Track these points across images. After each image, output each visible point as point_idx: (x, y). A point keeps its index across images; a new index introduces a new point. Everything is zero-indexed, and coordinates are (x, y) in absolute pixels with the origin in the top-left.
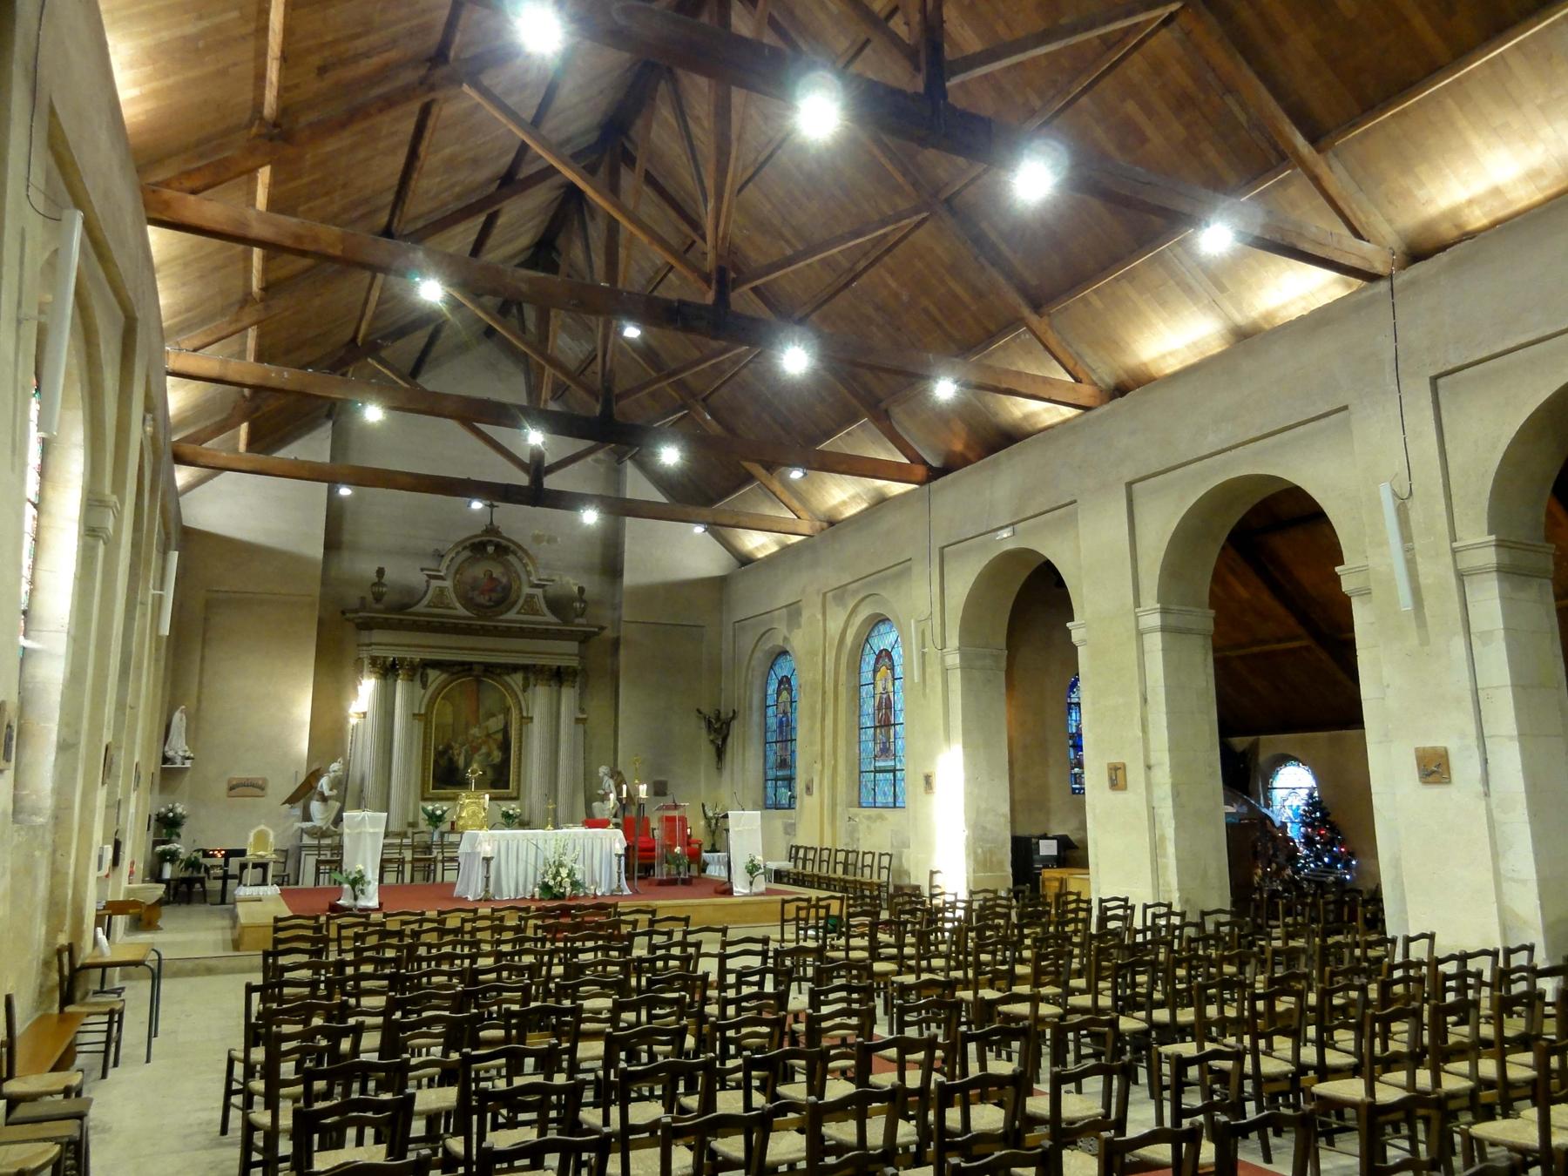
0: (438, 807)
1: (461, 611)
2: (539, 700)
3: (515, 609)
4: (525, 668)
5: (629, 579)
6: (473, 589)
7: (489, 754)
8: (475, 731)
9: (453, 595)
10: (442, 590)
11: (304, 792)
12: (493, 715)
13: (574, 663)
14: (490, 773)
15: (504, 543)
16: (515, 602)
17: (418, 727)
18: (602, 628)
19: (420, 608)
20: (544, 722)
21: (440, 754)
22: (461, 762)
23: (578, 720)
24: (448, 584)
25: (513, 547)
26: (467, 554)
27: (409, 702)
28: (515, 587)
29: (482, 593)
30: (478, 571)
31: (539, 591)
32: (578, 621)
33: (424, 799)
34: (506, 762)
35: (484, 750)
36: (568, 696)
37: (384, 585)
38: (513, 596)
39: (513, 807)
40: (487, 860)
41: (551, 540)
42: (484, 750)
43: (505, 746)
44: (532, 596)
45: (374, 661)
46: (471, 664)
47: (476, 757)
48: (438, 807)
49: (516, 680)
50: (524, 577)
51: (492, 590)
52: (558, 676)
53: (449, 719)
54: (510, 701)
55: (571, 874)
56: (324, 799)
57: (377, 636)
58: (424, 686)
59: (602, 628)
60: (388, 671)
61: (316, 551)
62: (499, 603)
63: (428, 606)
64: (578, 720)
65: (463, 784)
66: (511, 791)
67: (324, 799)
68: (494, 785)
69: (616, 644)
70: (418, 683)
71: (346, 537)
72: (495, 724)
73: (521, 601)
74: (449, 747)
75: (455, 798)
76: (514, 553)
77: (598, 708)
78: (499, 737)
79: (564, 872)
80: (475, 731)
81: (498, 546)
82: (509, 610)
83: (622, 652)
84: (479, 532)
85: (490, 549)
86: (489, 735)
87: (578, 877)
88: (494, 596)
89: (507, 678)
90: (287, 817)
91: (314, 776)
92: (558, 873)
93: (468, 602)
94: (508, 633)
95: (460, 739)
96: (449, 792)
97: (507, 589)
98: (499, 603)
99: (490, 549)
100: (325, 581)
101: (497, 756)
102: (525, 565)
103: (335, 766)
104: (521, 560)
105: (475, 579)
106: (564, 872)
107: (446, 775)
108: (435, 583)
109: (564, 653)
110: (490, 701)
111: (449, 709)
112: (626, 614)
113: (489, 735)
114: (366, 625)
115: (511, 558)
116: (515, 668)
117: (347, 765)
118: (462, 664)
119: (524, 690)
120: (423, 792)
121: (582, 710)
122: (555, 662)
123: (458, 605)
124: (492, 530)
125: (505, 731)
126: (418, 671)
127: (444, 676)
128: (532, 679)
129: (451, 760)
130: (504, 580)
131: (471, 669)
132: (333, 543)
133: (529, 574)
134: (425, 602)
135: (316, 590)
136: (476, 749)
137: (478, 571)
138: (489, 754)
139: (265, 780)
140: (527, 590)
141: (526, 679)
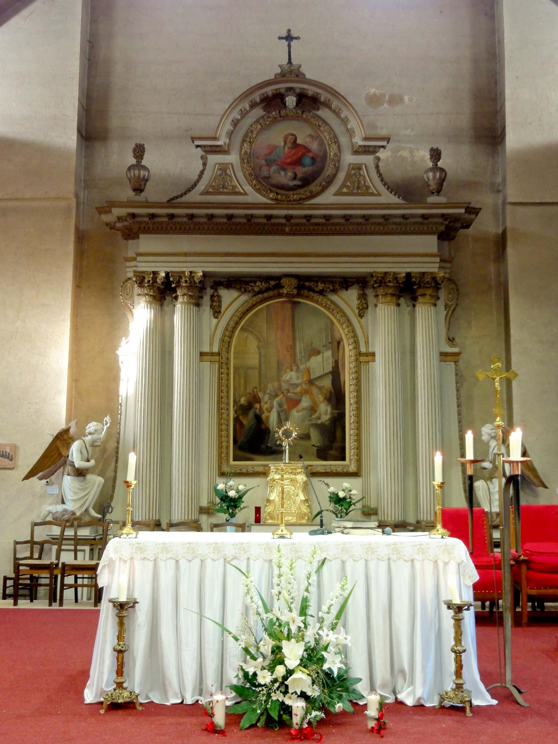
0: (233, 486)
1: (254, 196)
2: (382, 325)
3: (333, 188)
4: (361, 282)
5: (514, 139)
6: (269, 163)
7: (313, 409)
8: (291, 376)
9: (240, 175)
10: (224, 168)
11: (53, 459)
12: (319, 353)
13: (432, 267)
14: (316, 438)
15: (311, 90)
16: (330, 182)
17: (209, 370)
18: (473, 211)
19: (194, 196)
20: (391, 355)
21: (243, 410)
22: (273, 418)
23: (444, 355)
24: (233, 158)
25: (324, 96)
26: (259, 112)
27: (194, 333)
28: (331, 154)
29: (283, 168)
30: (276, 137)
31: (368, 159)
32: (432, 199)
33: (222, 474)
34: (339, 419)
35: (305, 403)
36: (427, 319)
37: (145, 168)
38: (329, 171)
39: (342, 486)
40: (123, 608)
41: (395, 100)
42: (305, 403)
43: (337, 398)
44: (358, 167)
45: (141, 280)
46: (278, 278)
47: (295, 414)
48: (233, 486)
49: (349, 298)
50: (344, 140)
51: (298, 162)
52: (408, 289)
53: (253, 360)
54: (342, 332)
55: (312, 657)
56: (80, 473)
57: (147, 243)
58: (217, 313)
59: (473, 211)
60: (163, 291)
61: (69, 139)
62: (306, 181)
63: (206, 193)
64: (444, 355)
65: (275, 452)
66: (349, 463)
67: (80, 473)
68: (322, 454)
69: (501, 242)
70: (207, 310)
71: (114, 123)
72: (320, 364)
73: (341, 176)
74: (255, 399)
75: (264, 474)
76: (327, 105)
77: (477, 337)
78: (327, 383)
79: (293, 653)
80: (291, 376)
81: (302, 97)
82: (324, 189)
83: (510, 251)
84: (270, 76)
85: (291, 101)
86: (311, 382)
87: (333, 664)
88: (301, 171)
89: (334, 298)
90: (44, 496)
91: (63, 439)
92: (277, 656)
93: (262, 182)
94: (328, 226)
95: (270, 386)
96: (257, 463)
97: (319, 160)
98: (306, 181)
99: (291, 101)
100: (86, 180)
101: (325, 412)
102: (345, 121)
103: (92, 426)
104: (337, 113)
105: (273, 148)
106: (293, 653)
107: (253, 441)
108: (213, 159)
109: (417, 253)
110: (311, 330)
111: (253, 344)
112: (513, 193)
113: (311, 382)
114: (131, 234)
115: (323, 113)
116: (345, 282)
117: (116, 423)
118: (267, 278)
119: (361, 316)
120: (220, 467)
121: (451, 340)
122: (402, 268)
123: (248, 188)
124: (291, 72)
125: (336, 374)
126: (206, 289)
127: (244, 298)
128: (371, 299)
129: (258, 418)
130: (314, 146)
131: (279, 286)
132: (92, 130)
133: (350, 133)
134: (201, 187)
135: (69, 188)
136: (295, 403)
137: (276, 137)
138: (313, 409)
139: (15, 448)
140: (349, 159)
141: (363, 297)
